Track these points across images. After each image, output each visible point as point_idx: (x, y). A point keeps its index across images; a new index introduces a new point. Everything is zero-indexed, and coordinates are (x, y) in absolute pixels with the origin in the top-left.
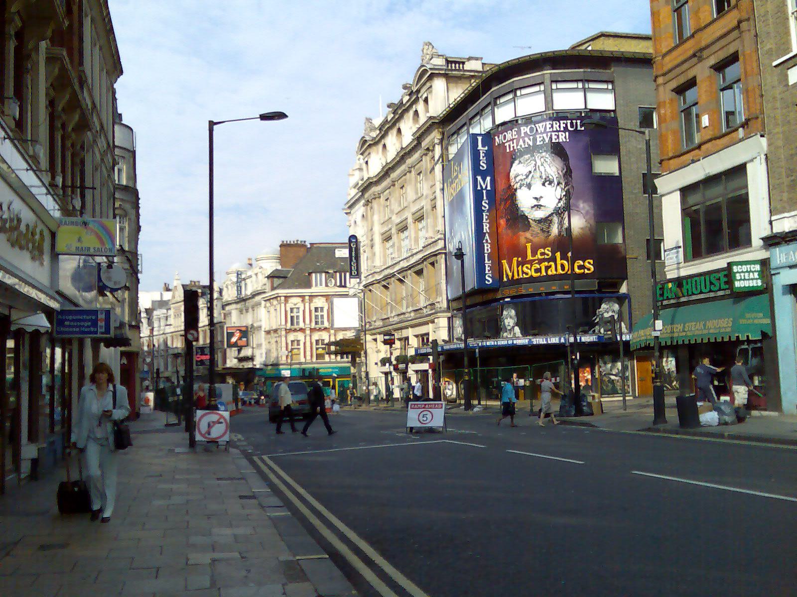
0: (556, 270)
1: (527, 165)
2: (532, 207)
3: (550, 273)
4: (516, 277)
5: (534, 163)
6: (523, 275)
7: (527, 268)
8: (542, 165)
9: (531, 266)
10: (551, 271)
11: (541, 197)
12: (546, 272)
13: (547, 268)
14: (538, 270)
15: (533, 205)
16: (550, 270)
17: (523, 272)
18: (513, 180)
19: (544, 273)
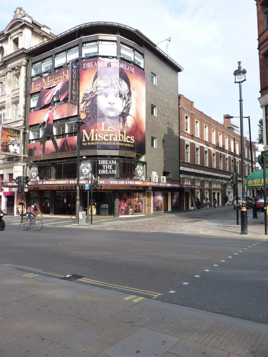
0: (118, 139)
1: (106, 82)
2: (107, 109)
3: (114, 140)
4: (93, 139)
5: (111, 81)
6: (98, 139)
7: (101, 135)
8: (116, 84)
9: (104, 135)
10: (115, 139)
11: (114, 103)
12: (112, 139)
13: (113, 137)
14: (106, 138)
15: (108, 107)
16: (115, 138)
17: (98, 138)
18: (95, 89)
19: (111, 140)
